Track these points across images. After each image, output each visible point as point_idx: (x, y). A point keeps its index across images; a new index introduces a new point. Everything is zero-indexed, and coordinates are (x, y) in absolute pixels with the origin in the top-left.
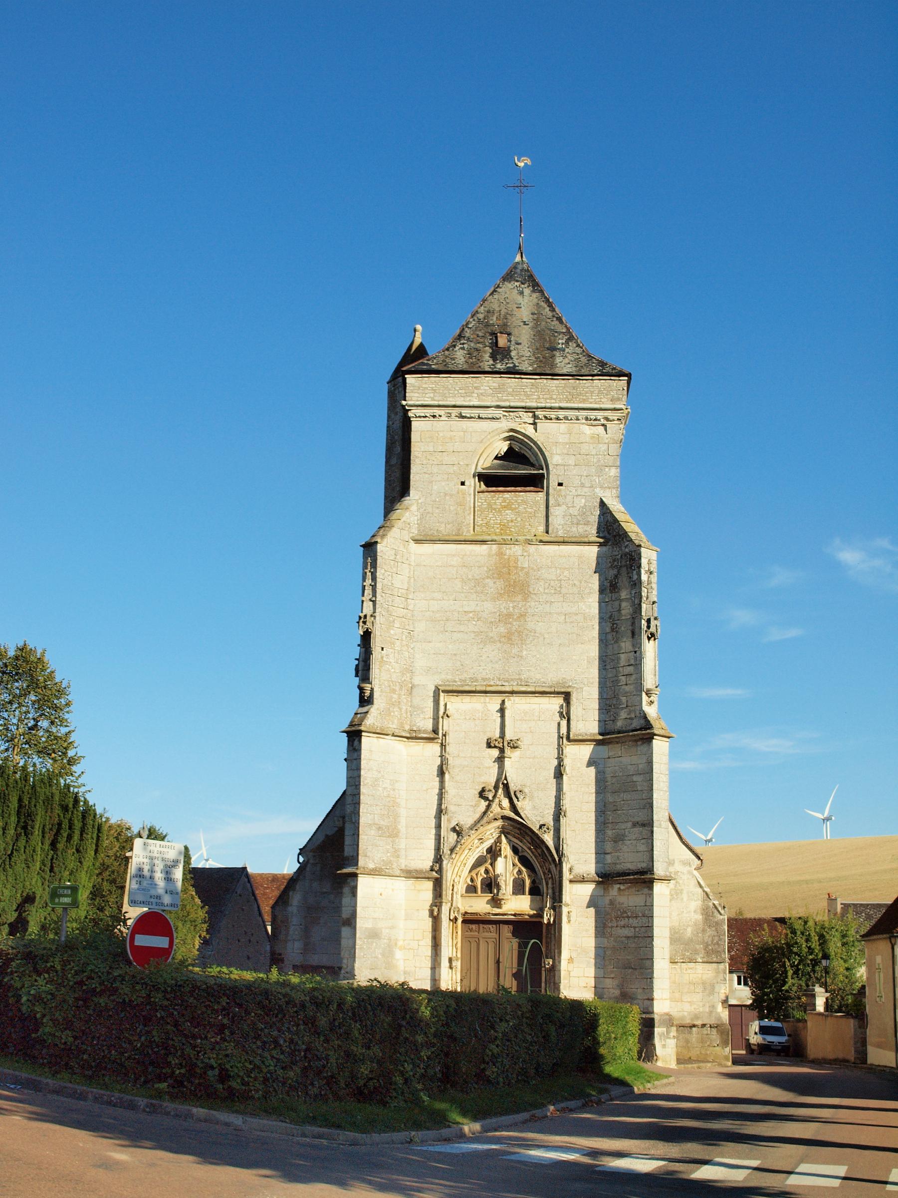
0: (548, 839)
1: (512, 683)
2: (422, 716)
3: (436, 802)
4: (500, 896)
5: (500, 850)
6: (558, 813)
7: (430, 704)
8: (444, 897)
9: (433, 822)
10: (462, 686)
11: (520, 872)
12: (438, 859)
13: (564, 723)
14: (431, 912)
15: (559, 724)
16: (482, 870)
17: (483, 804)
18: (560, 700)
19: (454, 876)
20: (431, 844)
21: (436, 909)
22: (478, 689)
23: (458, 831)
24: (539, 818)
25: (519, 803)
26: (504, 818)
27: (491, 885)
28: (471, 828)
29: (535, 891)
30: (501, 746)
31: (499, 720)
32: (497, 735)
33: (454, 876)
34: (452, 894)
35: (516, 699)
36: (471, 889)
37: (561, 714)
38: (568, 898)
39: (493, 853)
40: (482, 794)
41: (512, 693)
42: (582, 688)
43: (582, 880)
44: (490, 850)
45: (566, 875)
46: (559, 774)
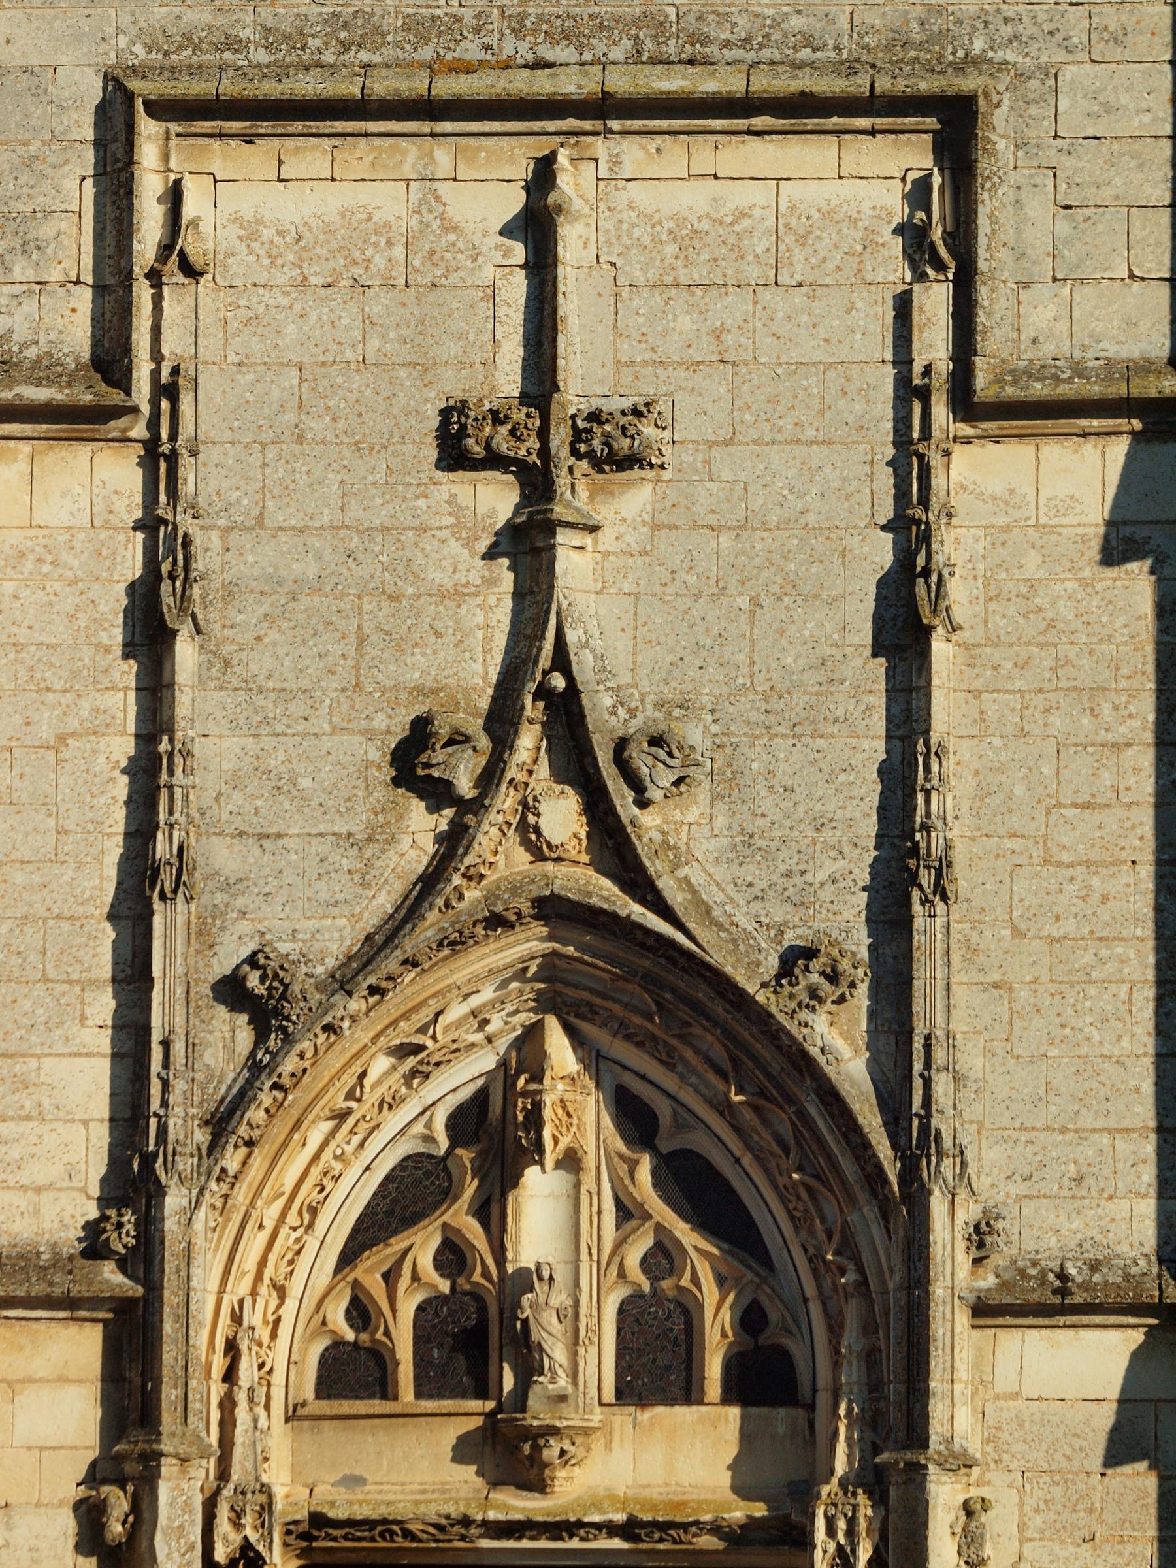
0: (839, 1040)
1: (599, 46)
2: (21, 270)
3: (118, 818)
4: (538, 1413)
5: (535, 1119)
6: (904, 870)
7: (75, 188)
8: (168, 1420)
9: (100, 948)
10: (280, 72)
11: (664, 1258)
12: (133, 1180)
13: (935, 300)
14: (90, 1516)
15: (903, 306)
16: (423, 1246)
17: (422, 826)
18: (913, 155)
19: (240, 1287)
20: (89, 1083)
21: (119, 1503)
22: (382, 86)
23: (258, 998)
24: (778, 912)
25: (649, 819)
26: (554, 910)
27: (478, 1341)
28: (343, 981)
29: (762, 1379)
30: (536, 450)
31: (517, 288)
32: (508, 380)
33: (240, 1287)
34: (228, 1405)
35: (629, 151)
36: (352, 1373)
37: (914, 238)
38: (964, 1420)
39: (497, 1134)
40: (412, 762)
41: (603, 109)
42: (1052, 73)
43: (1051, 1300)
44: (469, 1121)
45: (953, 1271)
46: (903, 626)
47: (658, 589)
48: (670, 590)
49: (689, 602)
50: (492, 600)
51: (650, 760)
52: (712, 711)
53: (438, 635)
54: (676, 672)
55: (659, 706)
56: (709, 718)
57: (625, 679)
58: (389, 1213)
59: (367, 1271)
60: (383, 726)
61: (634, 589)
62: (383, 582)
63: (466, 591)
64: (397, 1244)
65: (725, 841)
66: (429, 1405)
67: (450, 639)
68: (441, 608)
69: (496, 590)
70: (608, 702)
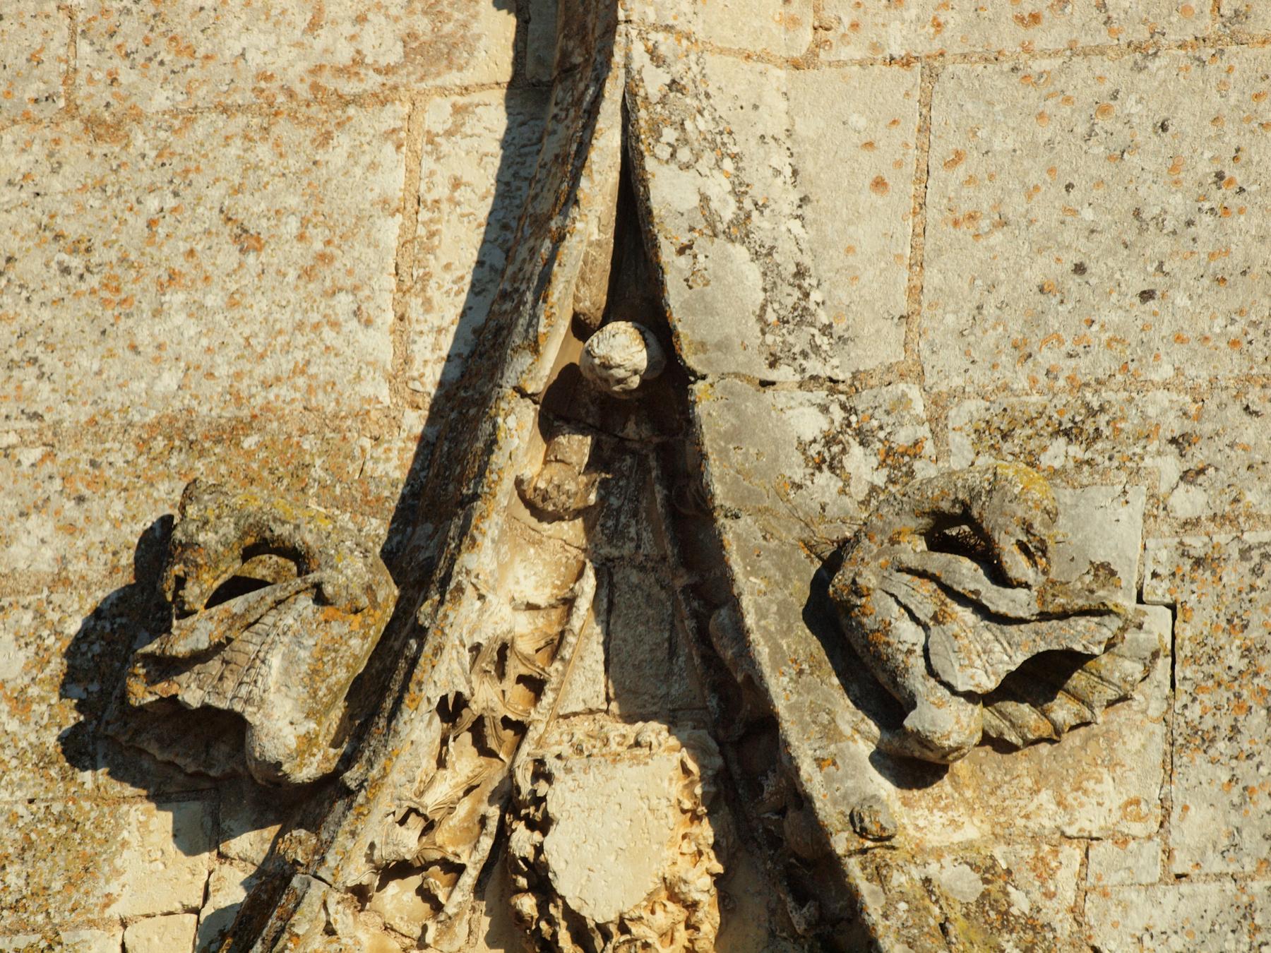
25: (935, 828)
47: (1008, 37)
48: (1047, 37)
49: (1113, 72)
50: (437, 115)
51: (924, 598)
52: (1180, 442)
53: (247, 240)
54: (1058, 317)
55: (992, 434)
56: (1169, 466)
57: (878, 348)
60: (45, 562)
61: (924, 45)
62: (69, 77)
63: (349, 87)
65: (1211, 895)
67: (286, 253)
68: (263, 152)
69: (453, 78)
70: (808, 422)
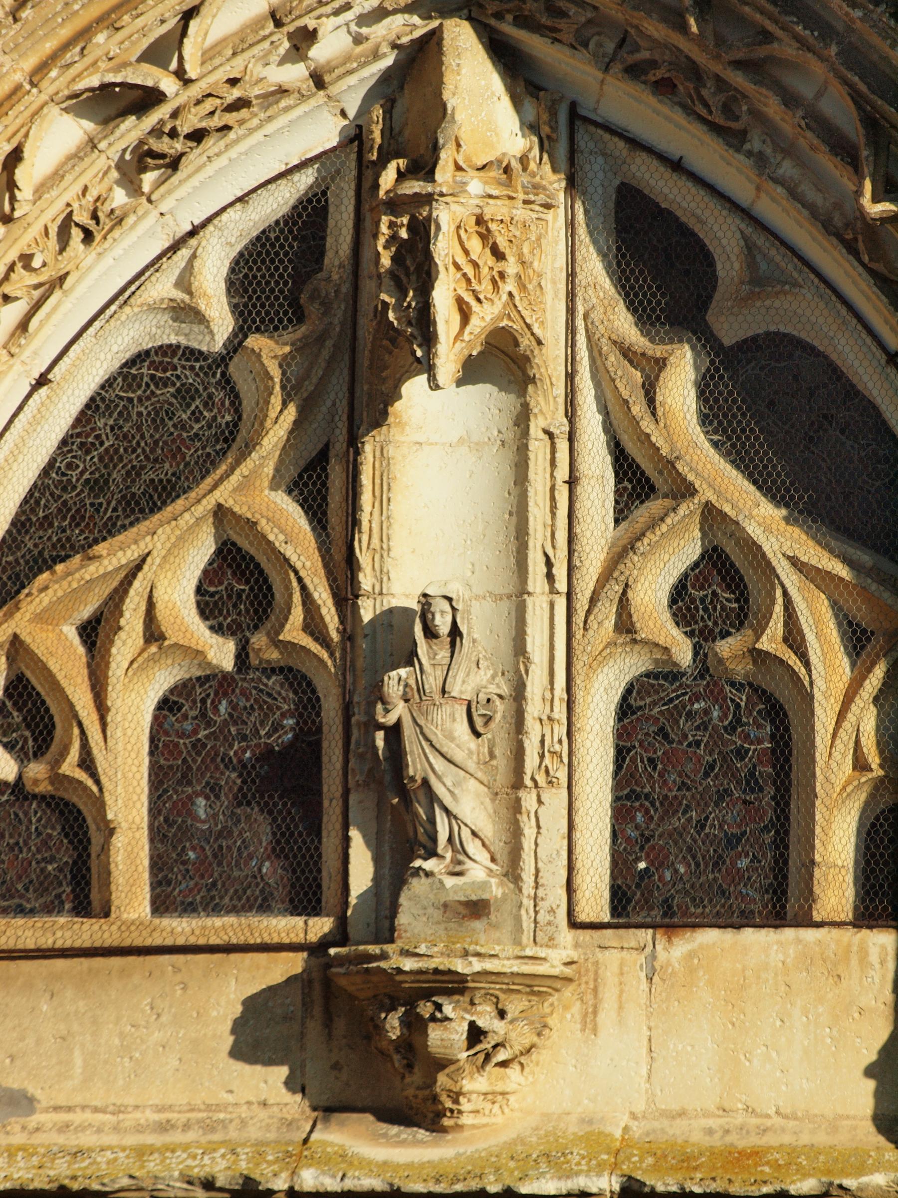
4: (421, 942)
5: (416, 265)
11: (722, 587)
16: (173, 559)
39: (337, 299)
58: (97, 486)
59: (40, 618)
64: (113, 556)
66: (181, 928)
